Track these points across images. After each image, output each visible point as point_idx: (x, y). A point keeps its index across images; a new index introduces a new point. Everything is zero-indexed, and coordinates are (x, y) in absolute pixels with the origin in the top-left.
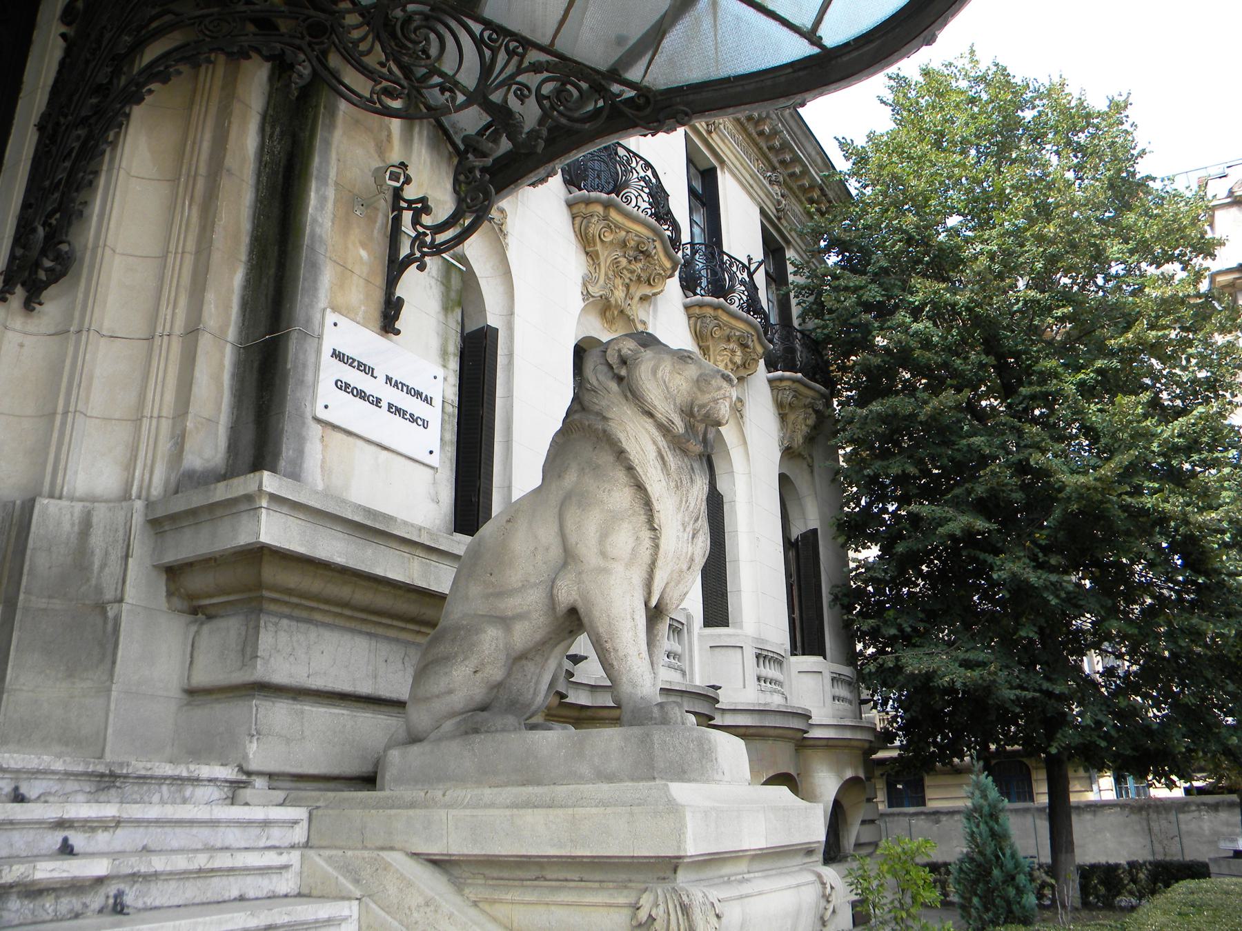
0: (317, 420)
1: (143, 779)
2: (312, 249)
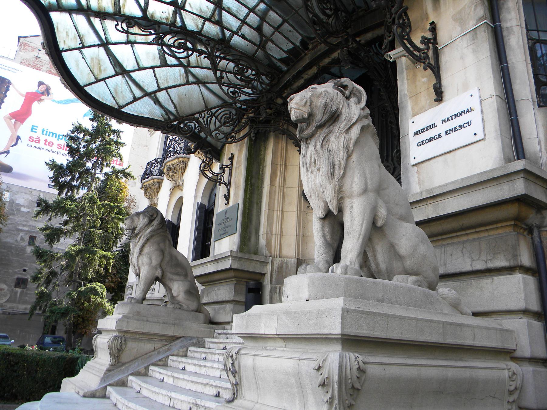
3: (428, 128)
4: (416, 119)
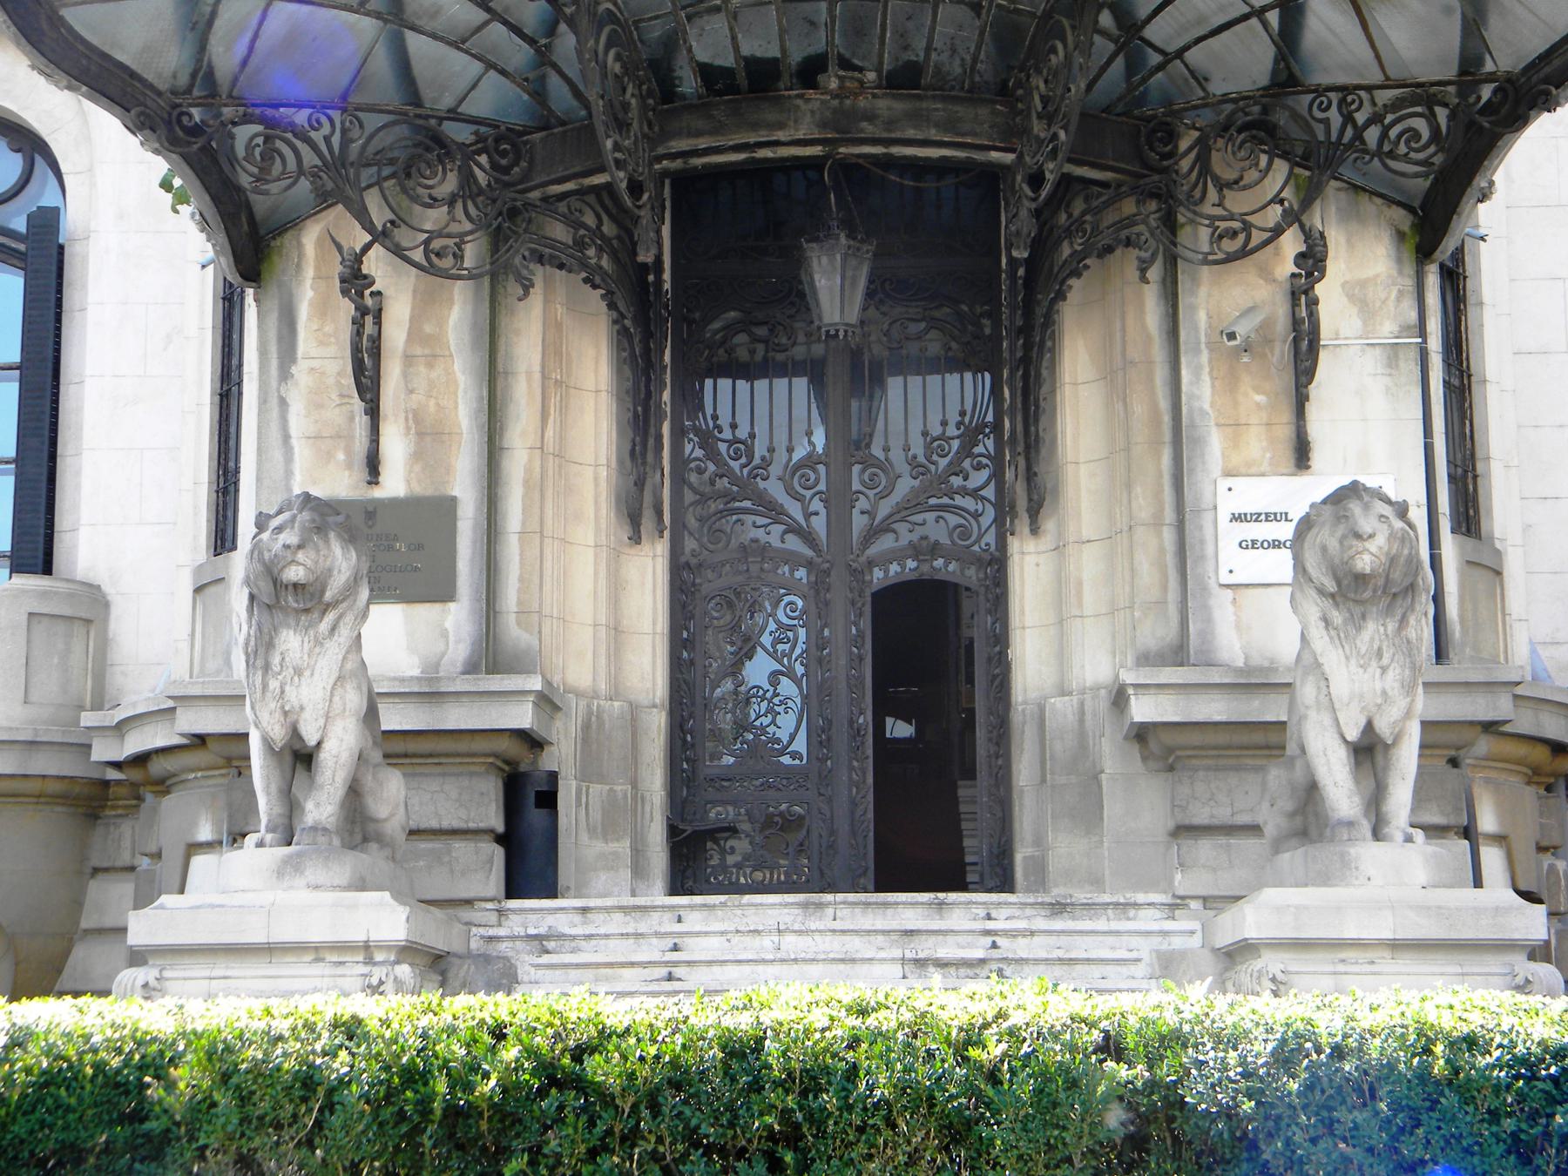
0: (1228, 586)
1: (1089, 906)
2: (1193, 426)
3: (1271, 517)
4: (1238, 483)
